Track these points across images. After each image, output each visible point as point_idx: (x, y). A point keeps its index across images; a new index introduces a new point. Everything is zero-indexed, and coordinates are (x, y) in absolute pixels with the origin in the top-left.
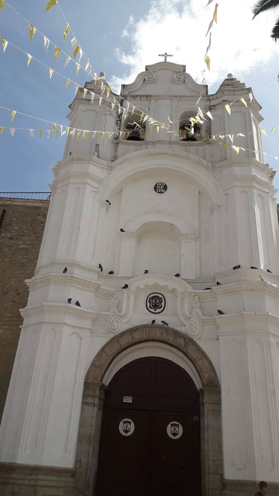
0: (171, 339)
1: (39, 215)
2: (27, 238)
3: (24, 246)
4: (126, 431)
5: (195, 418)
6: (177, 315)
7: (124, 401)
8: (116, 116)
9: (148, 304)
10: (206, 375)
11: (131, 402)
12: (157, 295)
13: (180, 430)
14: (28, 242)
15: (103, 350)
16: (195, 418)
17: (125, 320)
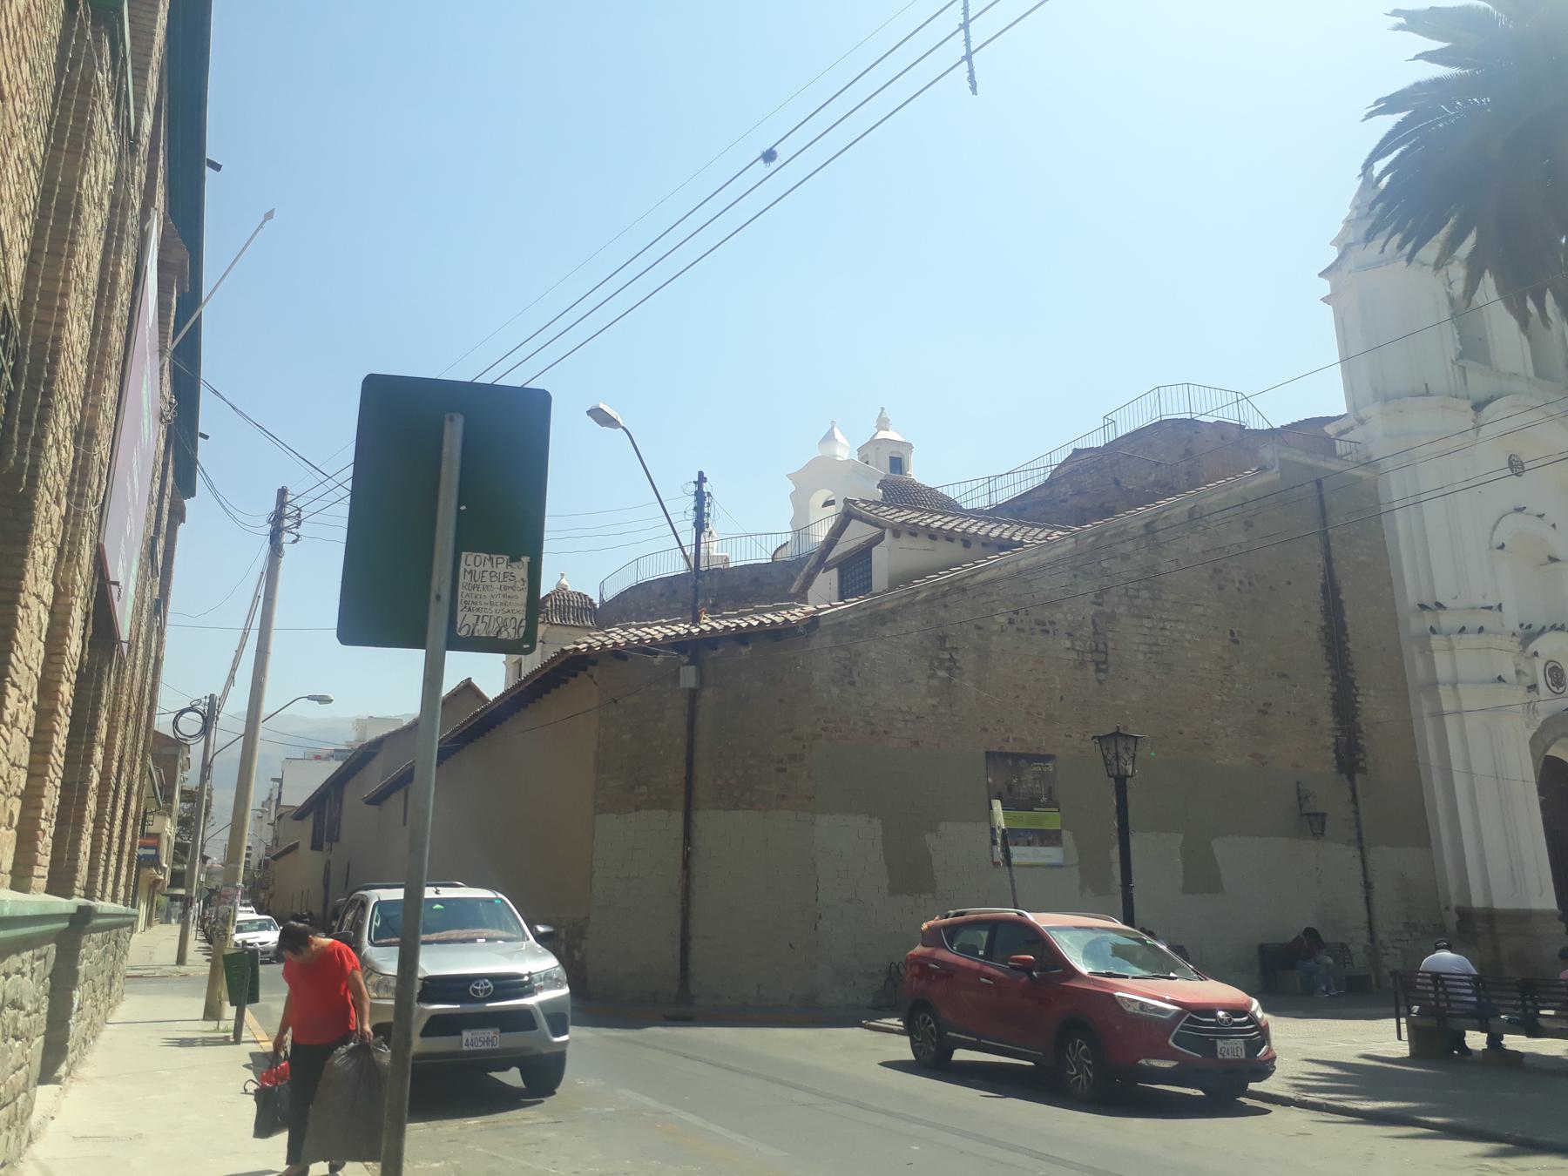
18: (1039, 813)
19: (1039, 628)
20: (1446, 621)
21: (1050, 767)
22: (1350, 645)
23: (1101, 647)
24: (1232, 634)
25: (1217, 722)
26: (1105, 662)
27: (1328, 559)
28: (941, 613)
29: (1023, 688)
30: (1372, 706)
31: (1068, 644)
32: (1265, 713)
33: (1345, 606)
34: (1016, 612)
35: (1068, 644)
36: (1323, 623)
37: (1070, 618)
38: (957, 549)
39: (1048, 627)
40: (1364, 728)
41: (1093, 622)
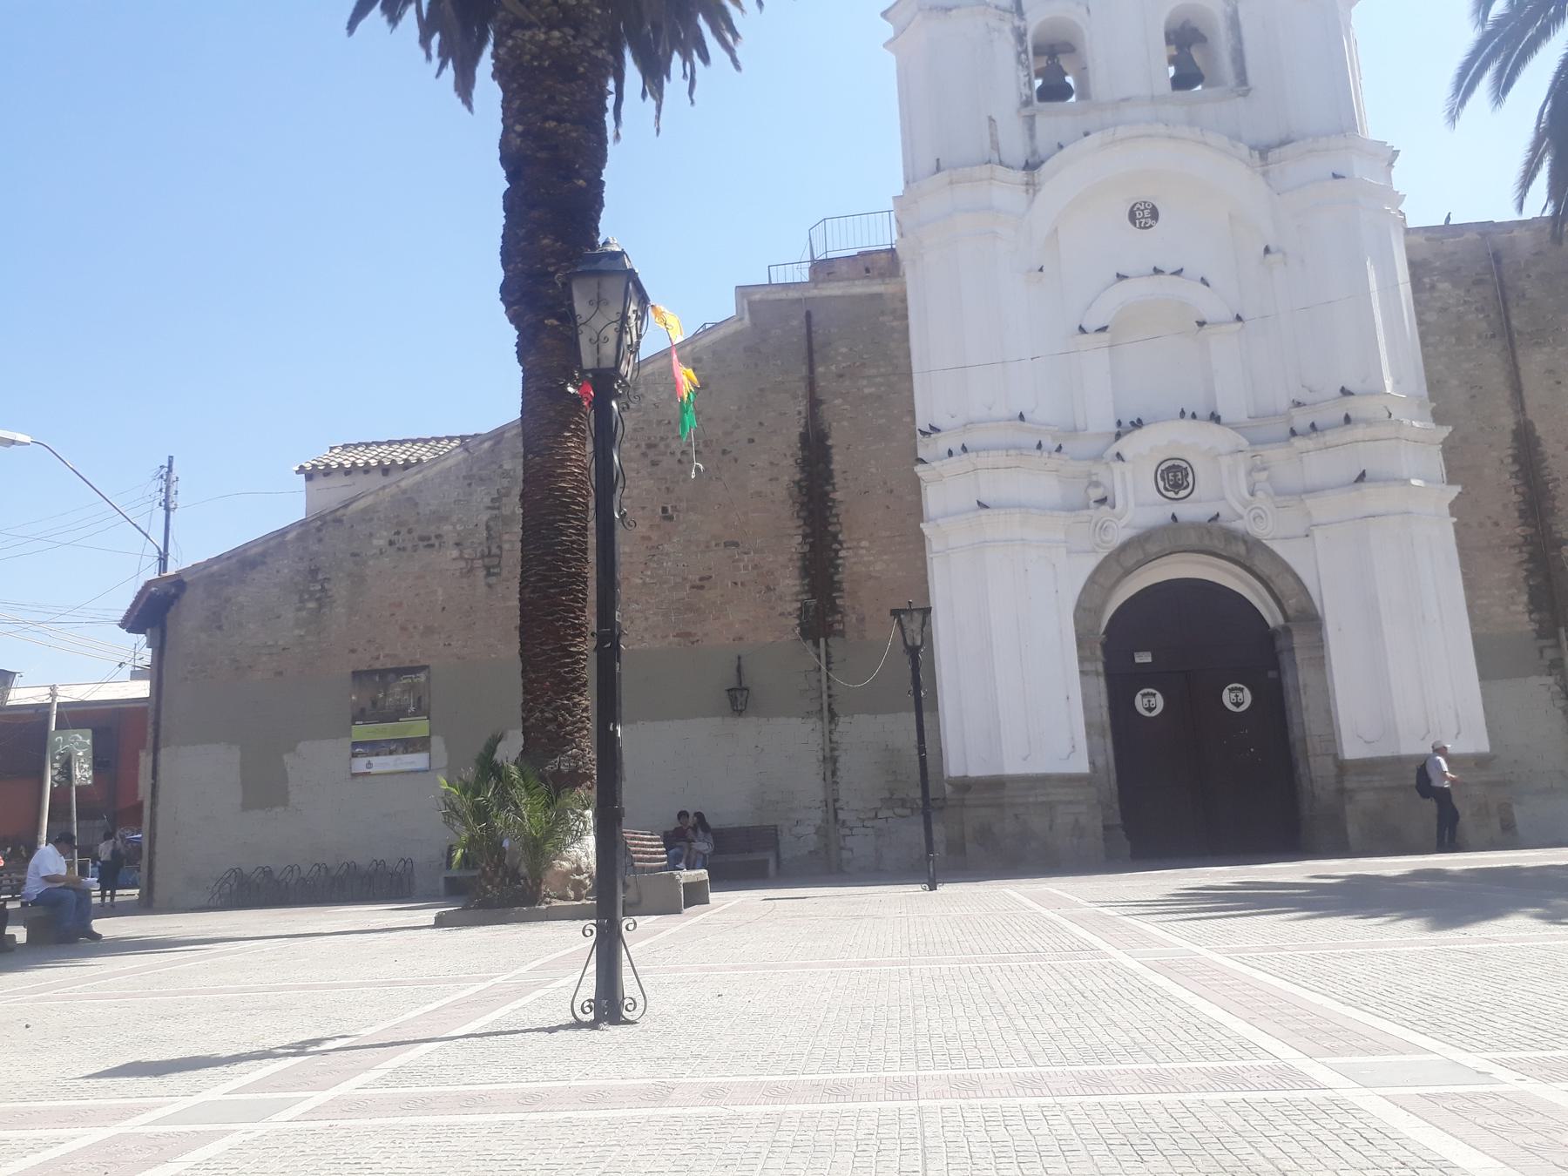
0: (1218, 545)
1: (883, 313)
2: (873, 371)
3: (873, 390)
4: (1150, 709)
5: (1272, 674)
6: (1223, 499)
7: (1138, 660)
8: (1012, 39)
9: (1161, 484)
10: (1292, 604)
11: (1149, 660)
12: (1177, 463)
13: (1247, 697)
14: (879, 380)
15: (1092, 579)
16: (1272, 674)
17: (1124, 522)
18: (404, 723)
19: (421, 544)
20: (943, 443)
21: (422, 677)
22: (837, 496)
23: (495, 550)
24: (664, 510)
25: (635, 606)
26: (499, 565)
27: (814, 403)
28: (315, 548)
29: (400, 604)
30: (863, 559)
31: (455, 553)
32: (702, 587)
33: (833, 451)
34: (398, 533)
35: (455, 553)
36: (797, 477)
37: (459, 527)
38: (377, 480)
39: (433, 541)
40: (845, 586)
41: (488, 528)
